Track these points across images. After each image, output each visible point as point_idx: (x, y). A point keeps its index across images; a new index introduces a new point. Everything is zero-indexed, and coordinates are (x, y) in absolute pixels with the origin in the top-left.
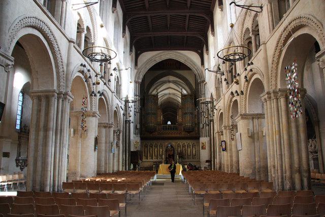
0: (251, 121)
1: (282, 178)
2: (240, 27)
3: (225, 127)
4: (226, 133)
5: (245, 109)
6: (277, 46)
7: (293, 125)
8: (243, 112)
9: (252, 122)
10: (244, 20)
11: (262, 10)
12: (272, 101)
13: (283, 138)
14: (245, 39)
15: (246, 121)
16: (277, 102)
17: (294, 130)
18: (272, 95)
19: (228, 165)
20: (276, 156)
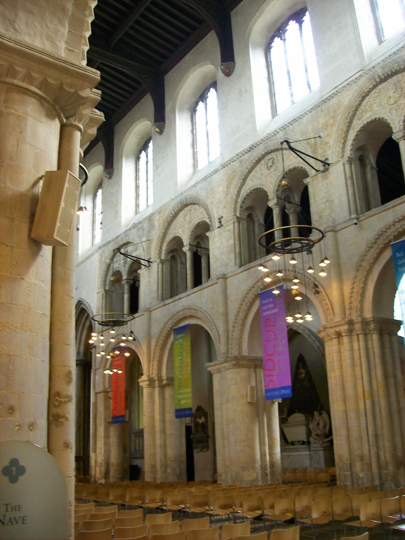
0: (252, 370)
1: (380, 478)
2: (236, 182)
3: (151, 381)
4: (151, 396)
5: (240, 345)
6: (375, 243)
7: (392, 381)
8: (234, 352)
9: (253, 374)
10: (250, 172)
11: (326, 170)
12: (355, 337)
13: (379, 404)
14: (243, 208)
15: (243, 372)
16: (366, 341)
17: (392, 391)
18: (358, 326)
19: (153, 466)
20: (365, 438)
